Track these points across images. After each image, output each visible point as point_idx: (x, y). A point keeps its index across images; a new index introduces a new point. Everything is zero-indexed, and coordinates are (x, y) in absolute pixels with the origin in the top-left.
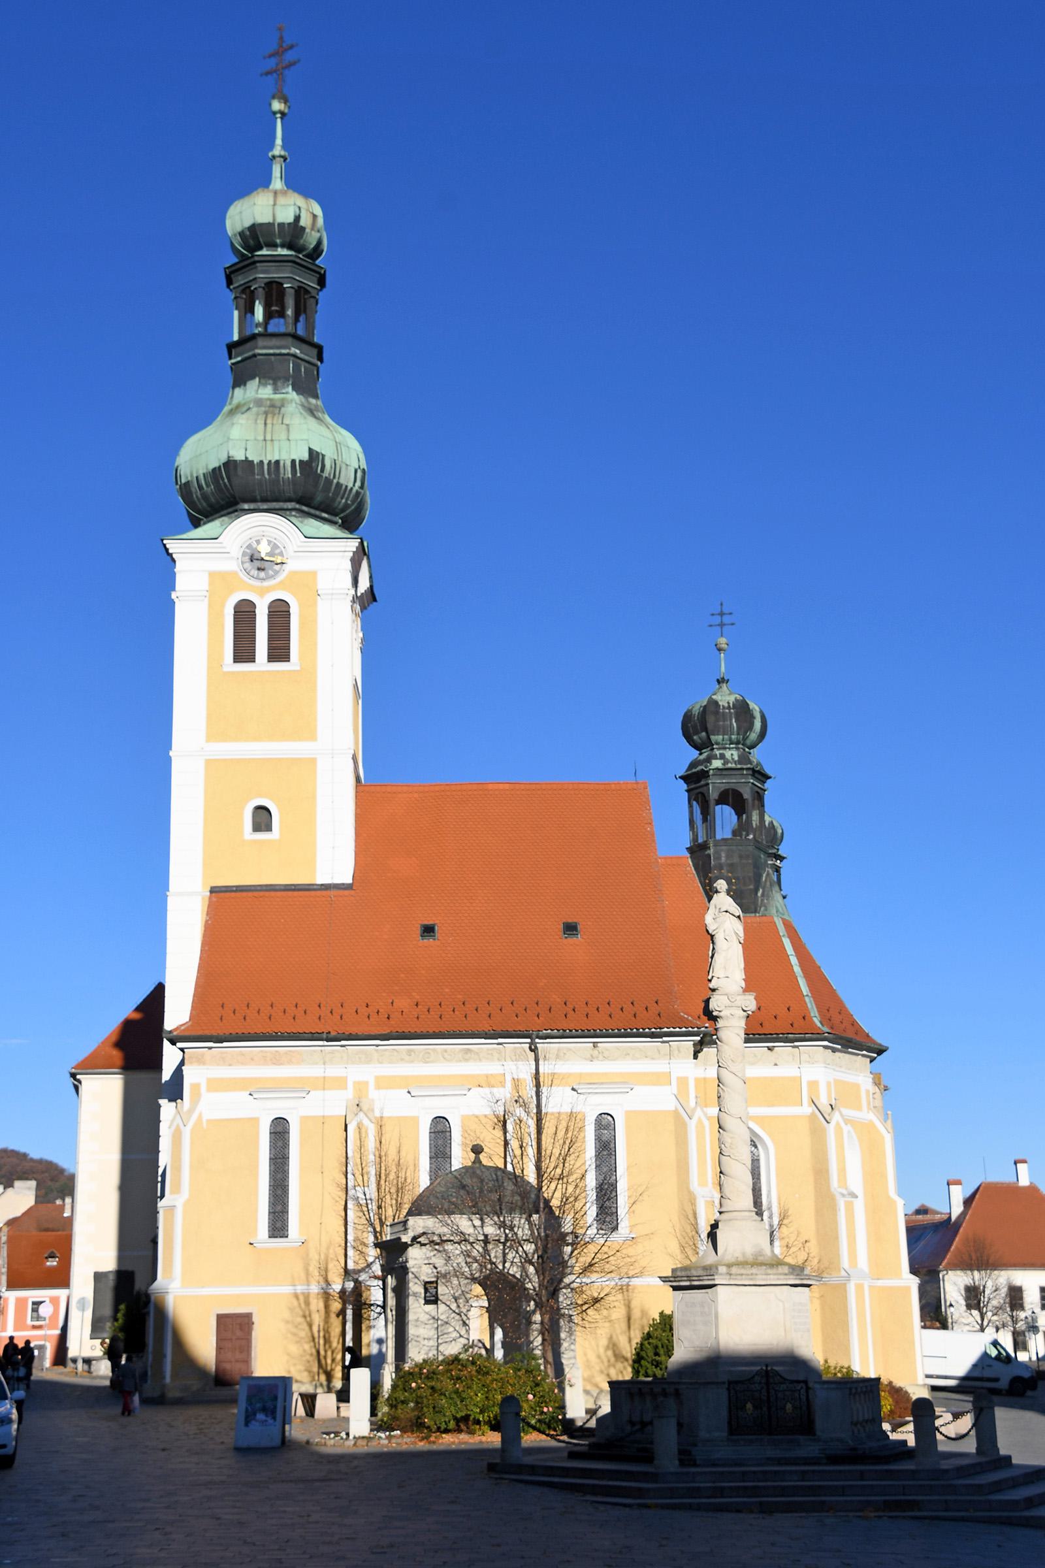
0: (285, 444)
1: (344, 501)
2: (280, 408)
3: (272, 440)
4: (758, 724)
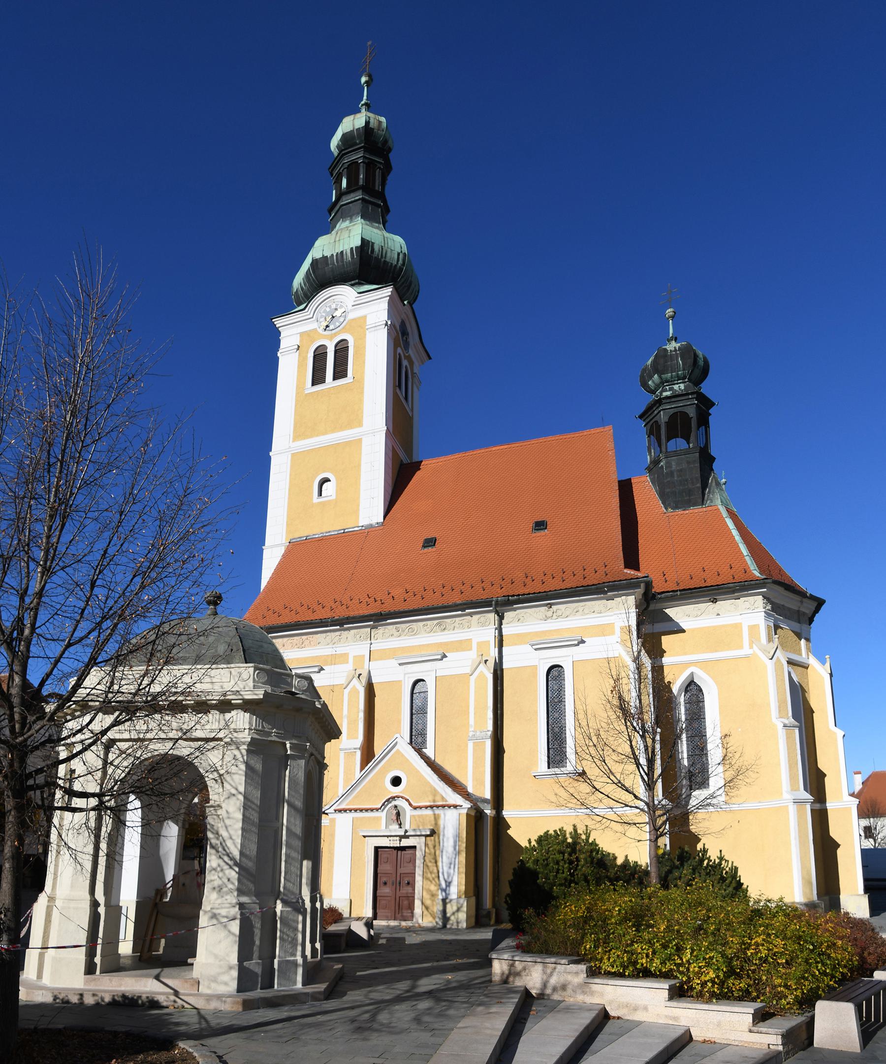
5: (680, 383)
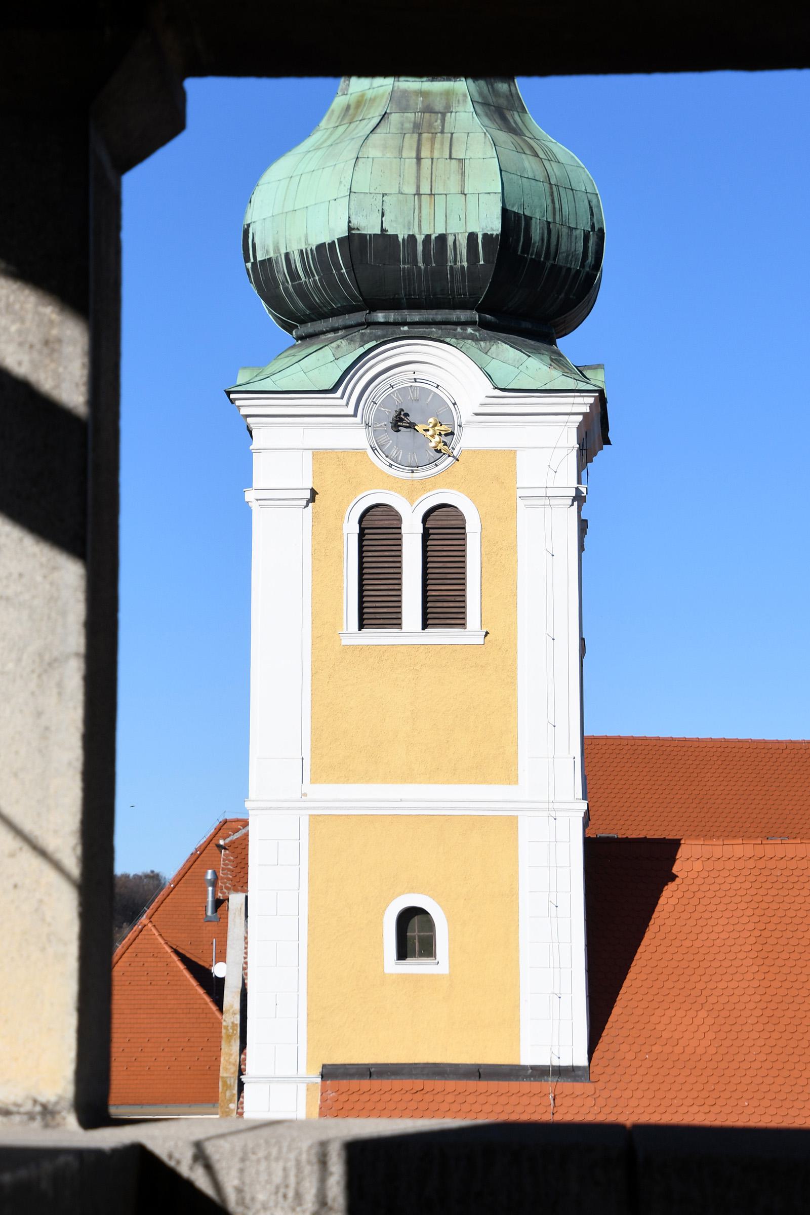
0: (456, 202)
1: (562, 296)
2: (444, 115)
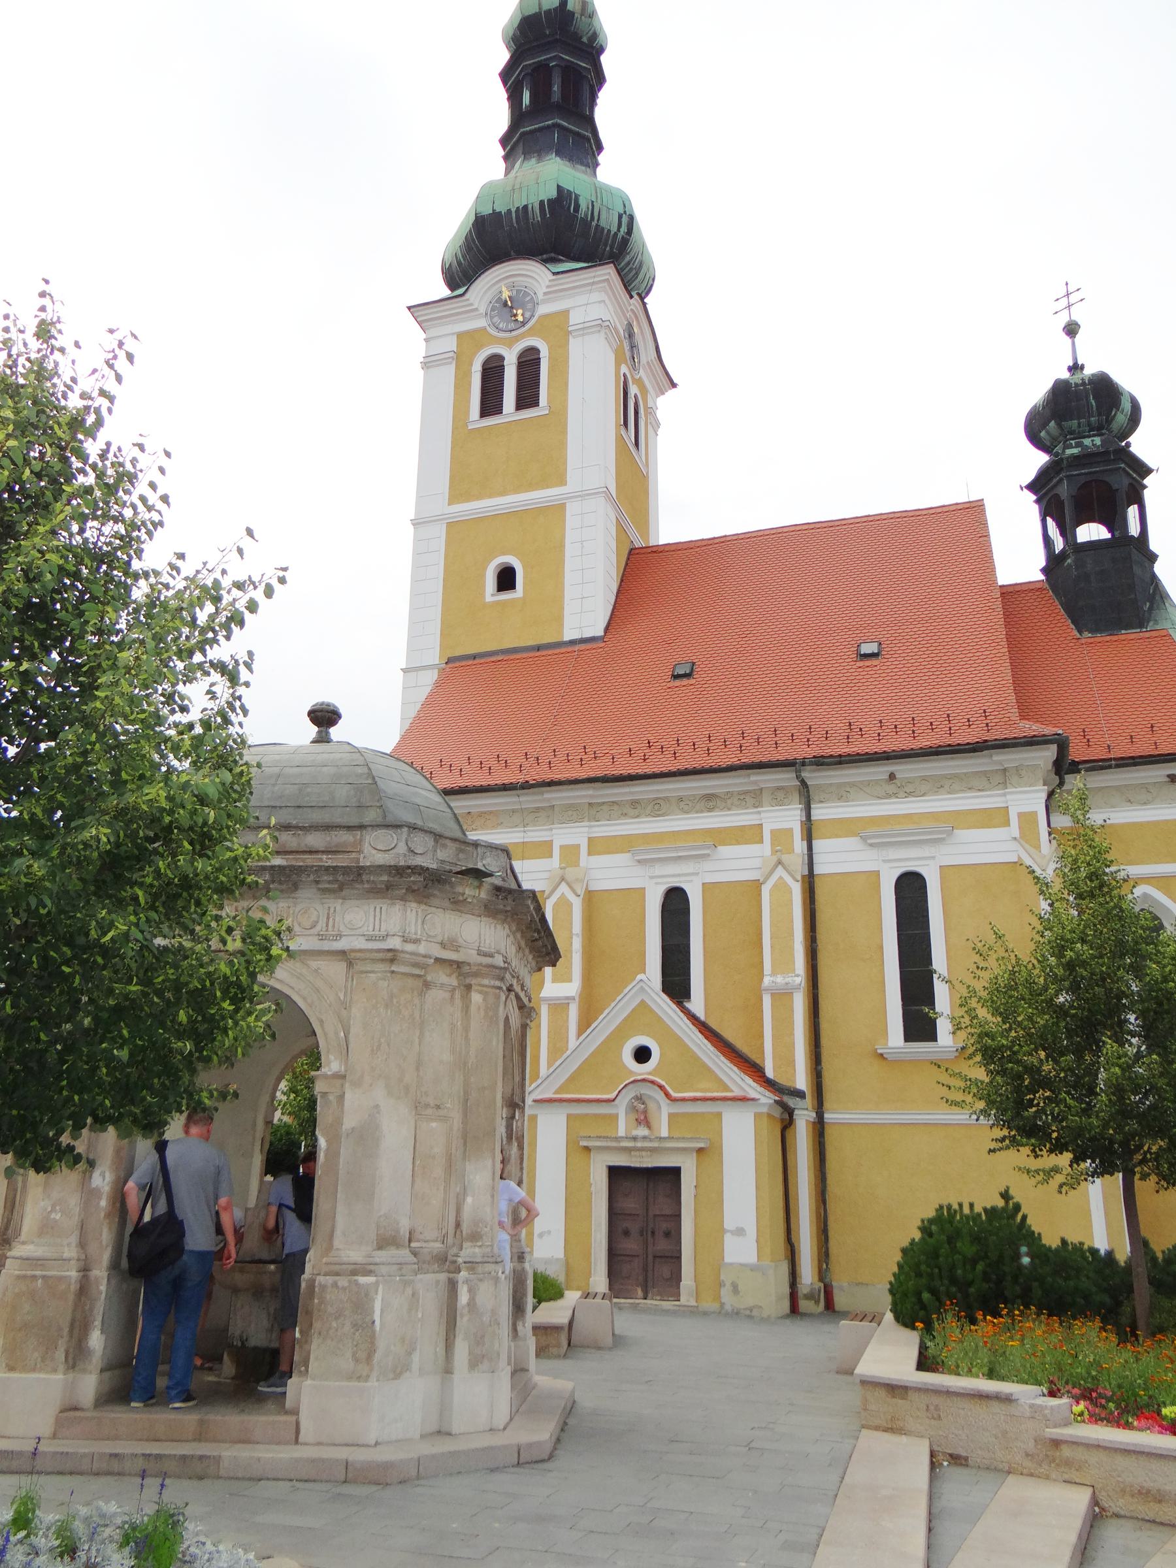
1: (608, 249)
3: (521, 188)
4: (1126, 405)
5: (1094, 436)
